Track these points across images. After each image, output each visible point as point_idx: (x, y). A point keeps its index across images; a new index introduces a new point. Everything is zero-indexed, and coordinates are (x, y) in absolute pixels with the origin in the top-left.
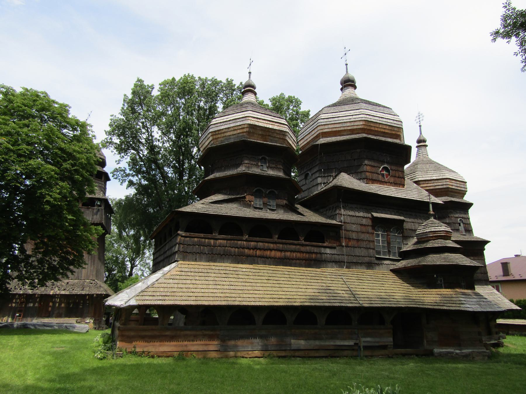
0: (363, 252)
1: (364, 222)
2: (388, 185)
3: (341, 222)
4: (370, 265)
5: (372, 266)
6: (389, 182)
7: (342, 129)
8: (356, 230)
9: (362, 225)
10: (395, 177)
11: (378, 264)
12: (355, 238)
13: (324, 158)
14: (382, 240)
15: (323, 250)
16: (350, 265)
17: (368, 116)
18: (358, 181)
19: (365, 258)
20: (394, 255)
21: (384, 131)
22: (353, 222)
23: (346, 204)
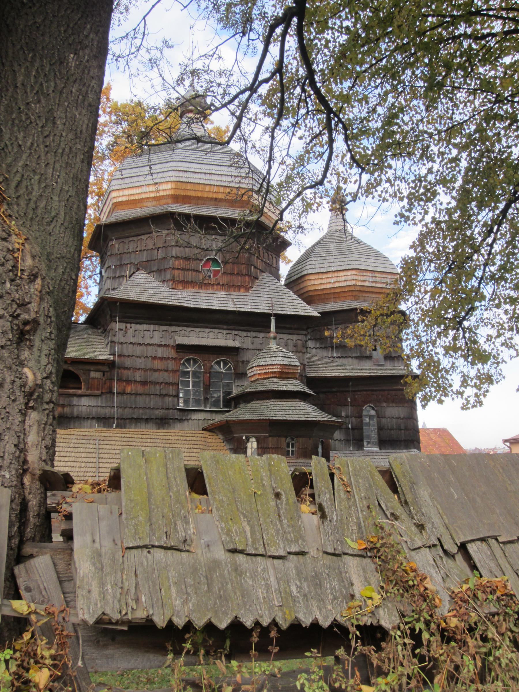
0: (153, 402)
1: (160, 352)
2: (217, 290)
3: (114, 355)
4: (163, 422)
5: (165, 423)
6: (219, 284)
7: (143, 196)
8: (143, 367)
9: (155, 358)
10: (232, 274)
11: (181, 420)
12: (138, 379)
13: (117, 246)
14: (194, 382)
15: (75, 401)
16: (123, 422)
17: (181, 174)
18: (161, 285)
19: (157, 412)
20: (216, 403)
21: (215, 196)
22: (138, 353)
23: (128, 325)
